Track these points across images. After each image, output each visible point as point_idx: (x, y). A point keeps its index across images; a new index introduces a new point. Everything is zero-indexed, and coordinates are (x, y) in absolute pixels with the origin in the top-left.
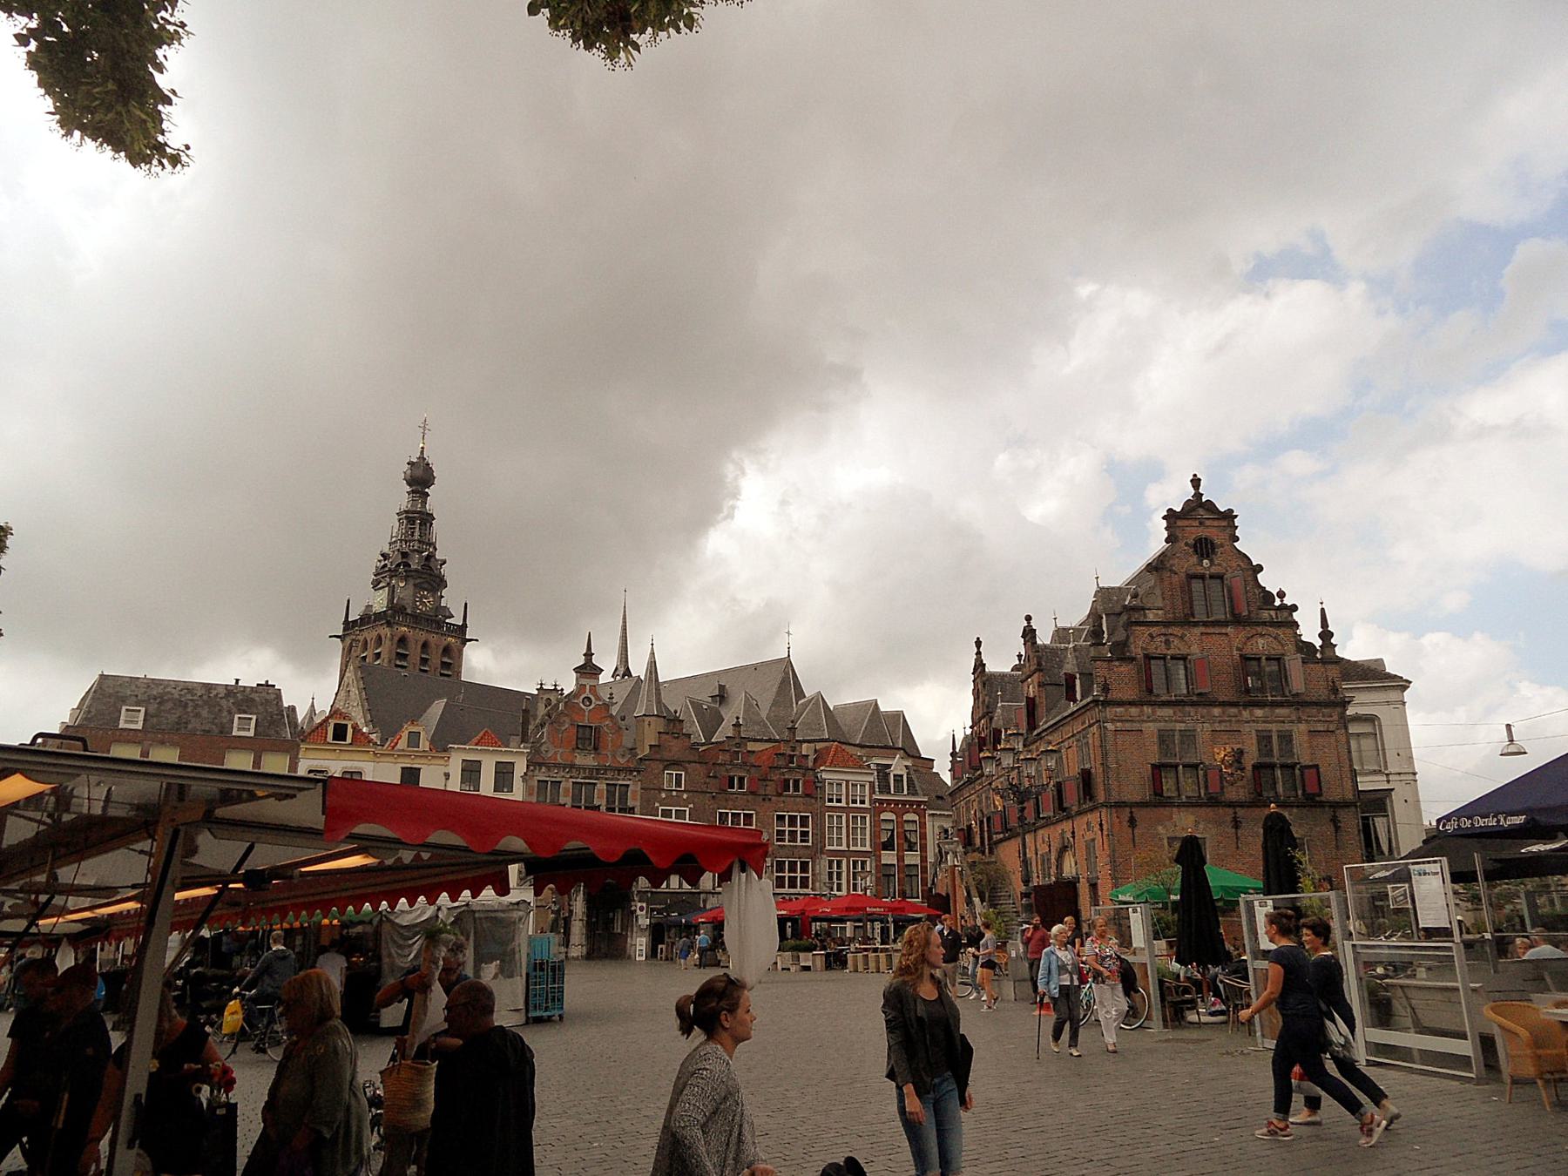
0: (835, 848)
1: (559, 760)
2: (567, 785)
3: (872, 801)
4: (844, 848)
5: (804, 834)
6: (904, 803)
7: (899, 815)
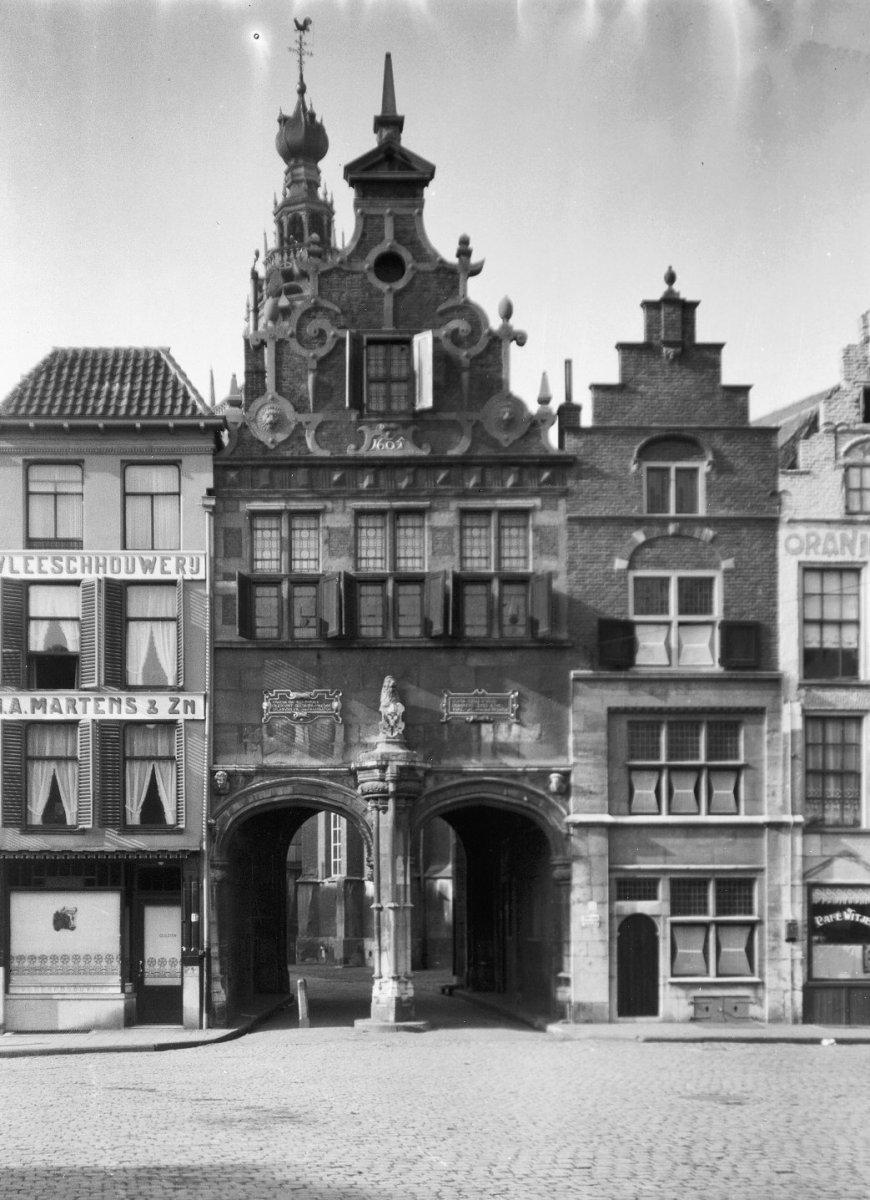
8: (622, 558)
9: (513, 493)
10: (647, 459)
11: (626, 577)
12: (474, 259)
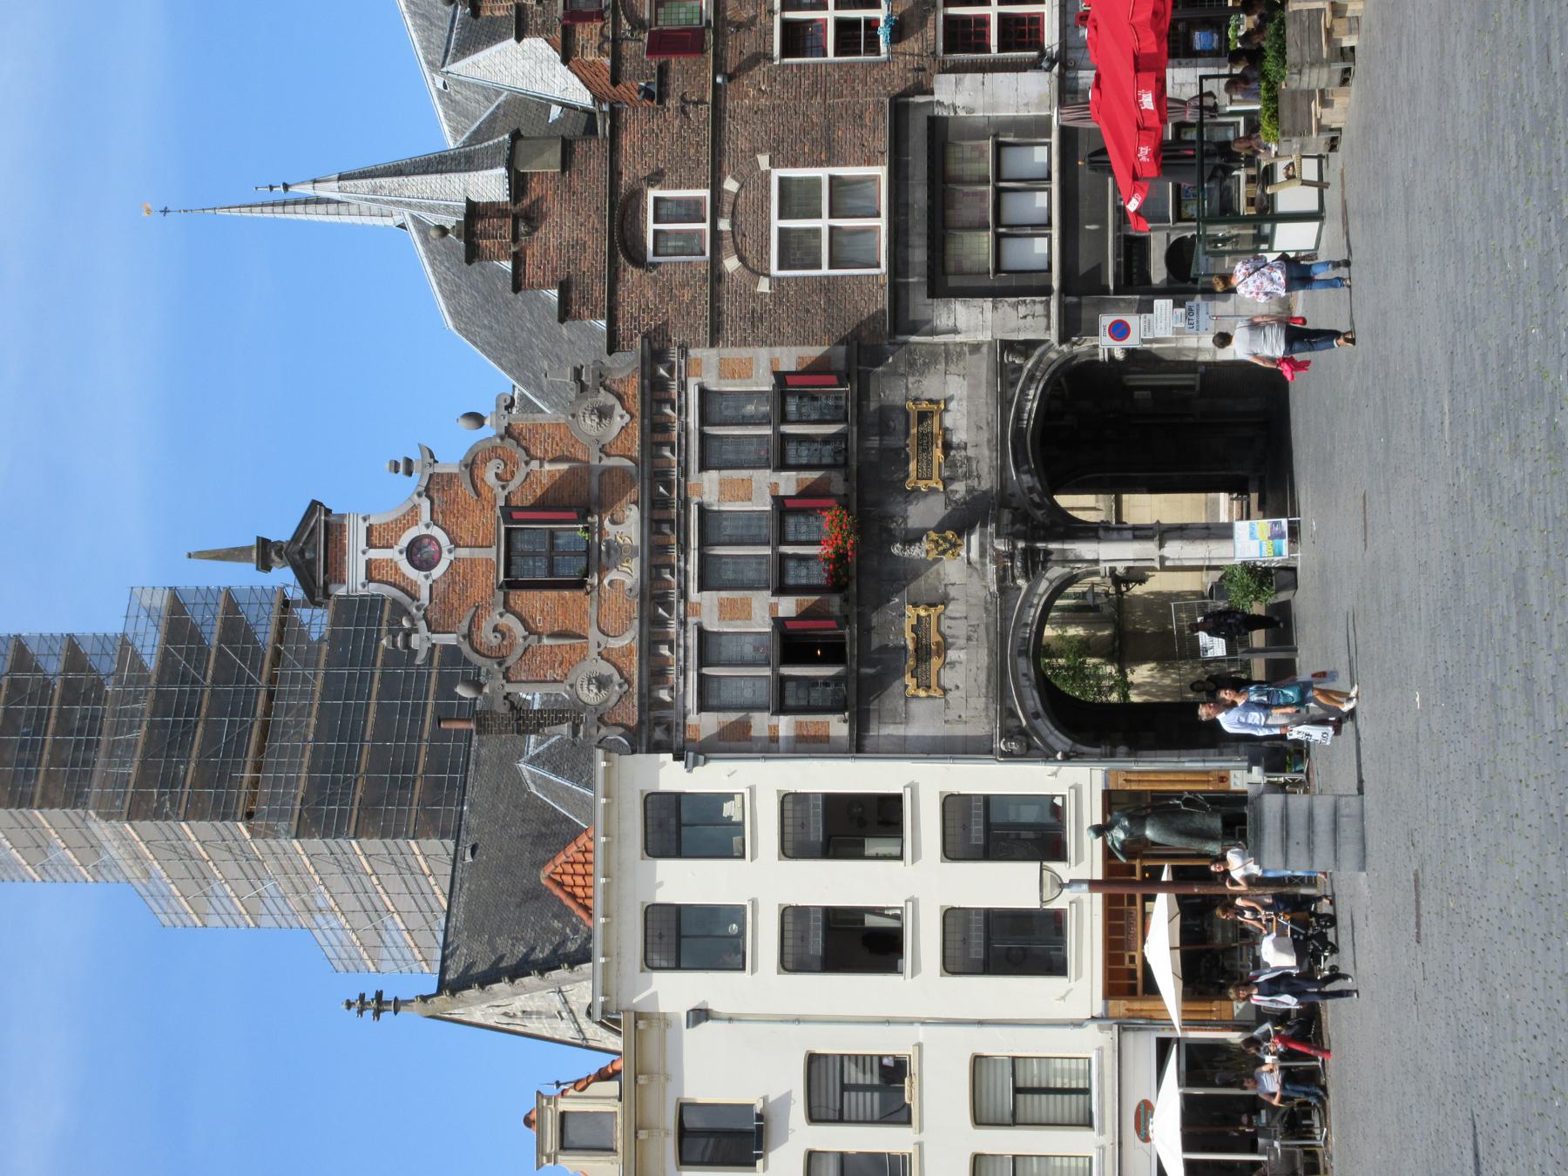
1: (628, 639)
2: (708, 608)
8: (757, 284)
9: (682, 410)
11: (779, 279)
12: (415, 456)
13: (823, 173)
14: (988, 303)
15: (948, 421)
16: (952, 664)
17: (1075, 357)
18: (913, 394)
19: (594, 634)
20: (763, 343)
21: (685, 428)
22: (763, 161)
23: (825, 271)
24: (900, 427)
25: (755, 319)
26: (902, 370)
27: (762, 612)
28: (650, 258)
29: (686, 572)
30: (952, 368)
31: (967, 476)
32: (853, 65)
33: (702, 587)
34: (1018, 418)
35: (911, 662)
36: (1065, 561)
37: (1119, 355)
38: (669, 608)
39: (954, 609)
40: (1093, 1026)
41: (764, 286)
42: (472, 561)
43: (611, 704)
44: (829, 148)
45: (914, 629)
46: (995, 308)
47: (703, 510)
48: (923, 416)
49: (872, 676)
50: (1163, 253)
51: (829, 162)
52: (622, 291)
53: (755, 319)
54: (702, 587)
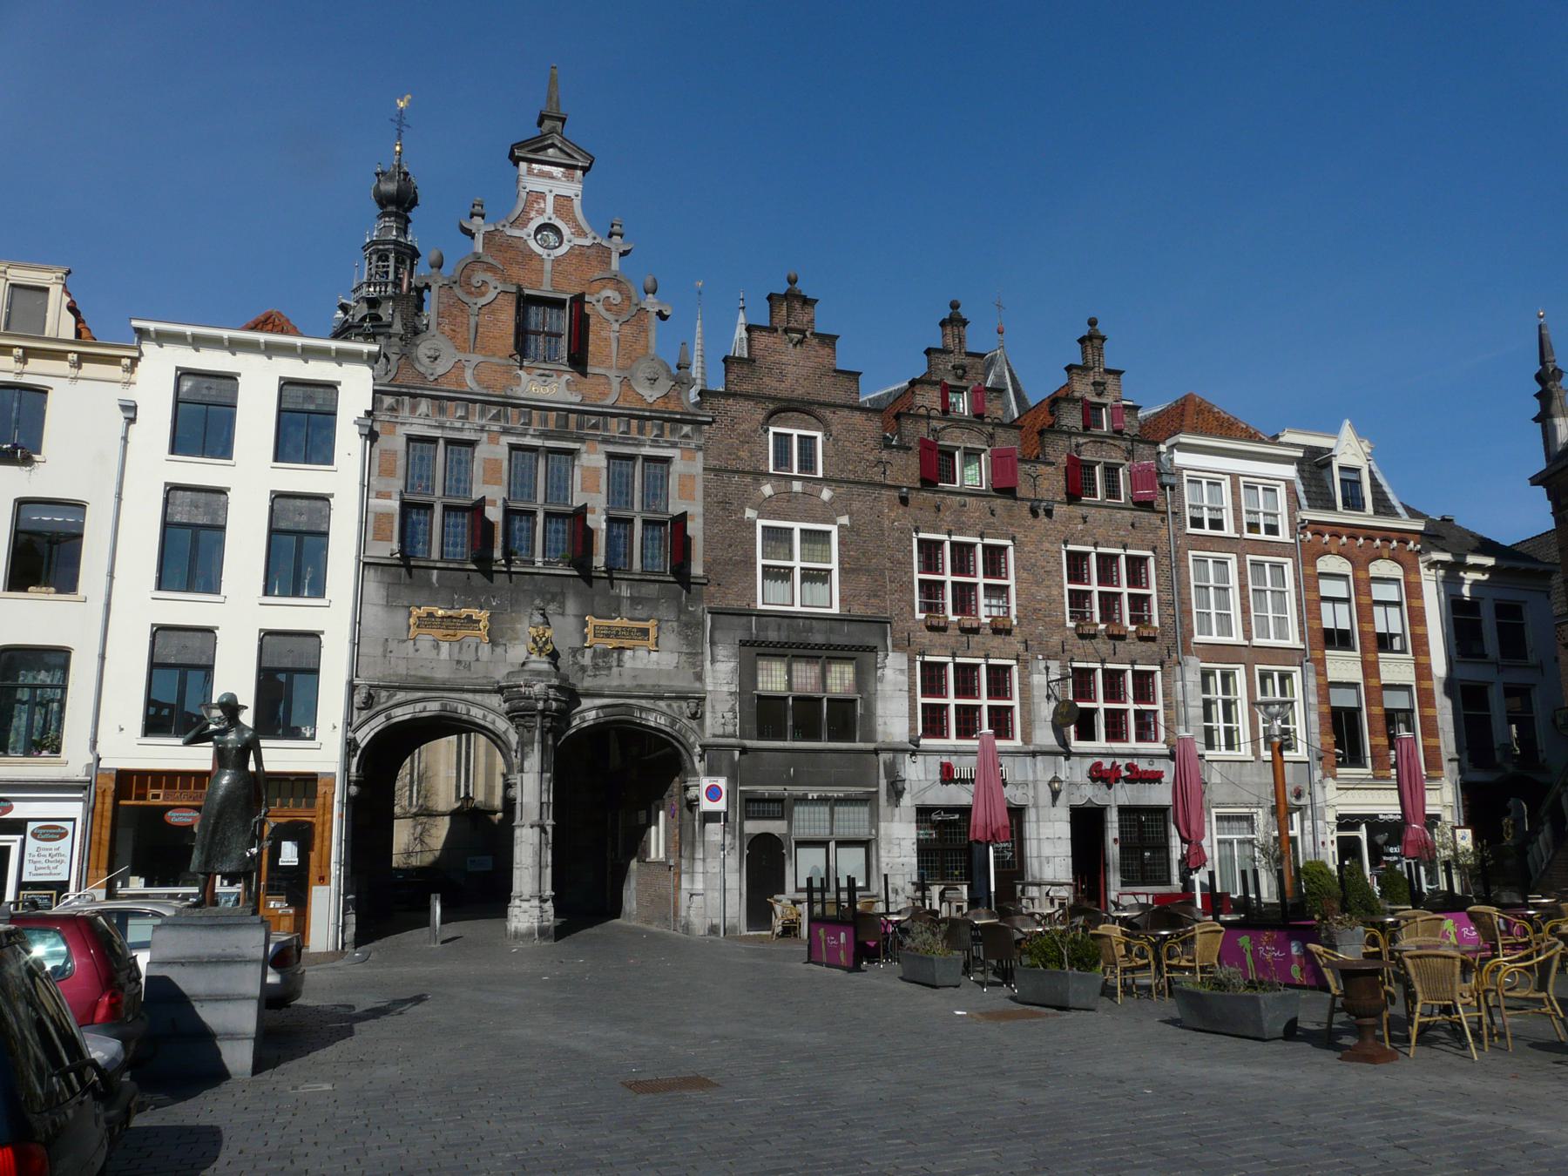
0: (1215, 638)
1: (470, 383)
2: (493, 451)
3: (1298, 527)
4: (1237, 638)
5: (1139, 602)
6: (1370, 532)
7: (1360, 562)
9: (655, 443)
10: (774, 425)
11: (754, 525)
13: (834, 566)
14: (734, 688)
15: (641, 653)
16: (437, 647)
17: (691, 756)
18: (664, 625)
19: (476, 358)
20: (706, 510)
21: (640, 444)
22: (844, 520)
23: (760, 562)
24: (637, 614)
25: (724, 504)
26: (683, 618)
27: (493, 496)
28: (772, 429)
29: (525, 435)
30: (683, 658)
31: (596, 667)
32: (912, 591)
33: (513, 447)
34: (642, 709)
35: (440, 612)
36: (524, 744)
37: (691, 794)
38: (496, 418)
39: (485, 649)
40: (90, 759)
41: (750, 513)
42: (542, 271)
43: (417, 365)
44: (853, 570)
45: (469, 617)
46: (731, 694)
47: (572, 453)
48: (645, 632)
49: (430, 579)
50: (770, 831)
51: (842, 570)
52: (749, 405)
53: (724, 504)
54: (513, 447)
